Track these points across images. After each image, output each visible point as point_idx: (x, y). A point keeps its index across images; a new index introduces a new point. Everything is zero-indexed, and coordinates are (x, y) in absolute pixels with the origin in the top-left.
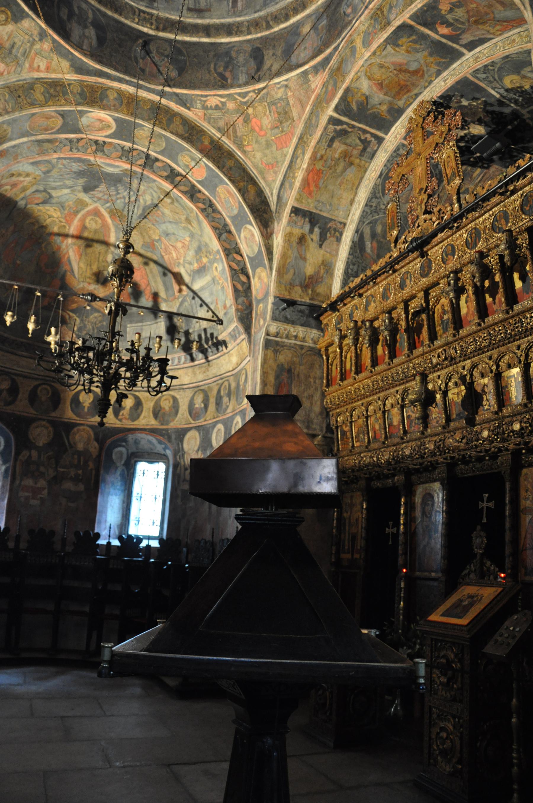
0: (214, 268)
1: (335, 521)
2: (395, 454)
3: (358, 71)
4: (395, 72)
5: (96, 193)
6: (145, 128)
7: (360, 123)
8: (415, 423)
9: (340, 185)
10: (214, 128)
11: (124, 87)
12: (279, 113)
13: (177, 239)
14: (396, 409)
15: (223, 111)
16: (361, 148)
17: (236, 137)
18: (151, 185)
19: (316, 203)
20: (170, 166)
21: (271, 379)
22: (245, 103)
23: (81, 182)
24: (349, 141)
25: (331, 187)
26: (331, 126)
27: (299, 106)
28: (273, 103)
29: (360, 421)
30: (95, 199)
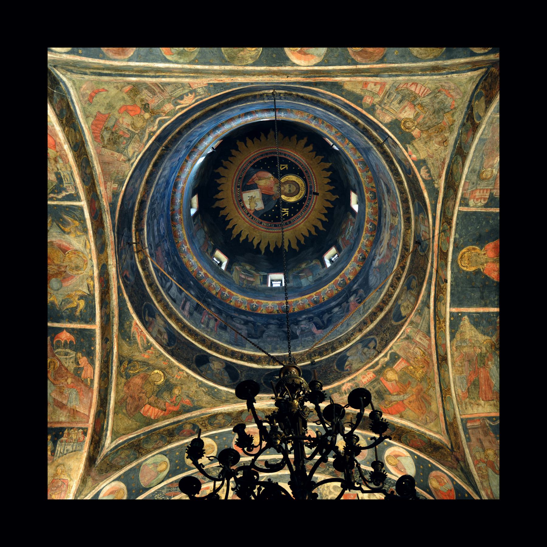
3: (90, 253)
4: (63, 269)
6: (251, 61)
17: (146, 88)
22: (156, 118)
26: (73, 192)
27: (107, 160)
28: (131, 138)
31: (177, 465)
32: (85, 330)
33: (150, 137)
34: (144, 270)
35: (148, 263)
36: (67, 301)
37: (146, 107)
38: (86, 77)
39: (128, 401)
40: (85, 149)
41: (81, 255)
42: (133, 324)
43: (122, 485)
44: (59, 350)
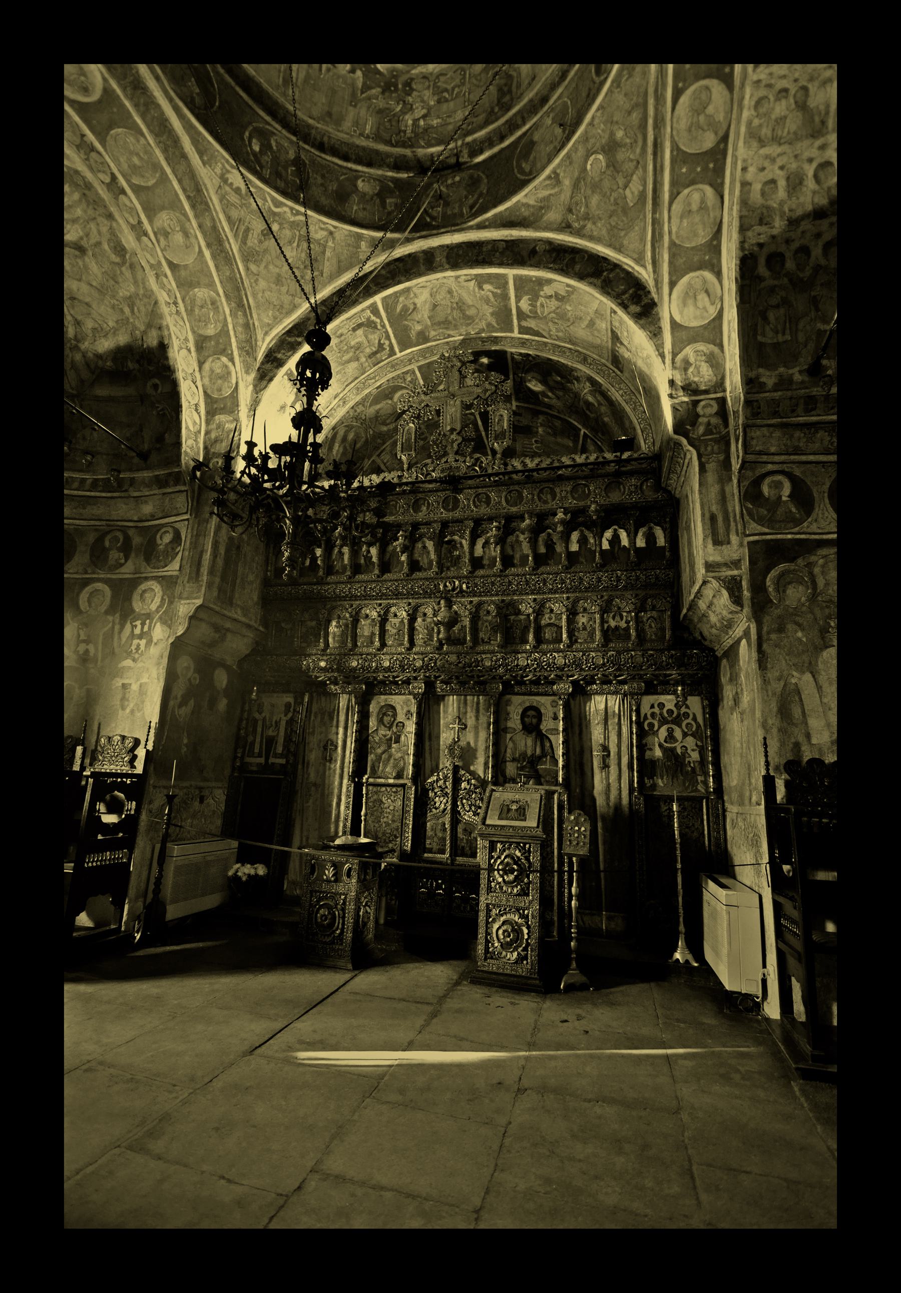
0: (149, 384)
1: (244, 722)
2: (367, 664)
6: (142, 141)
7: (391, 326)
8: (395, 639)
13: (89, 314)
14: (369, 621)
15: (244, 202)
16: (374, 349)
17: (245, 244)
18: (100, 220)
21: (222, 550)
22: (275, 214)
24: (371, 337)
29: (314, 623)
31: (705, 169)
32: (515, 285)
33: (298, 213)
34: (481, 152)
35: (475, 141)
36: (487, 301)
38: (256, 324)
39: (613, 224)
40: (329, 297)
41: (435, 290)
42: (524, 201)
43: (685, 280)
44: (539, 311)
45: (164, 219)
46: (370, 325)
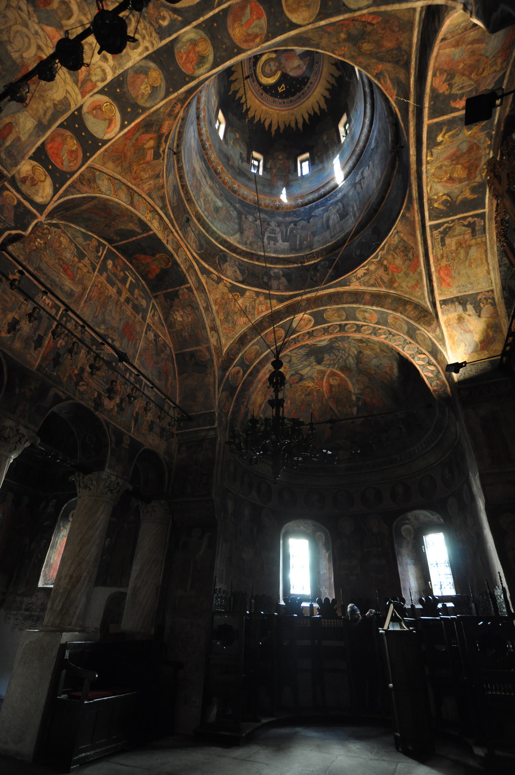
3: (427, 183)
4: (454, 162)
5: (326, 361)
7: (456, 215)
9: (470, 265)
10: (369, 286)
11: (309, 295)
12: (402, 251)
17: (385, 283)
19: (458, 289)
20: (355, 324)
23: (312, 359)
24: (457, 232)
25: (463, 272)
26: (434, 232)
28: (396, 248)
30: (327, 366)
37: (386, 269)
45: (359, 315)
46: (445, 233)
